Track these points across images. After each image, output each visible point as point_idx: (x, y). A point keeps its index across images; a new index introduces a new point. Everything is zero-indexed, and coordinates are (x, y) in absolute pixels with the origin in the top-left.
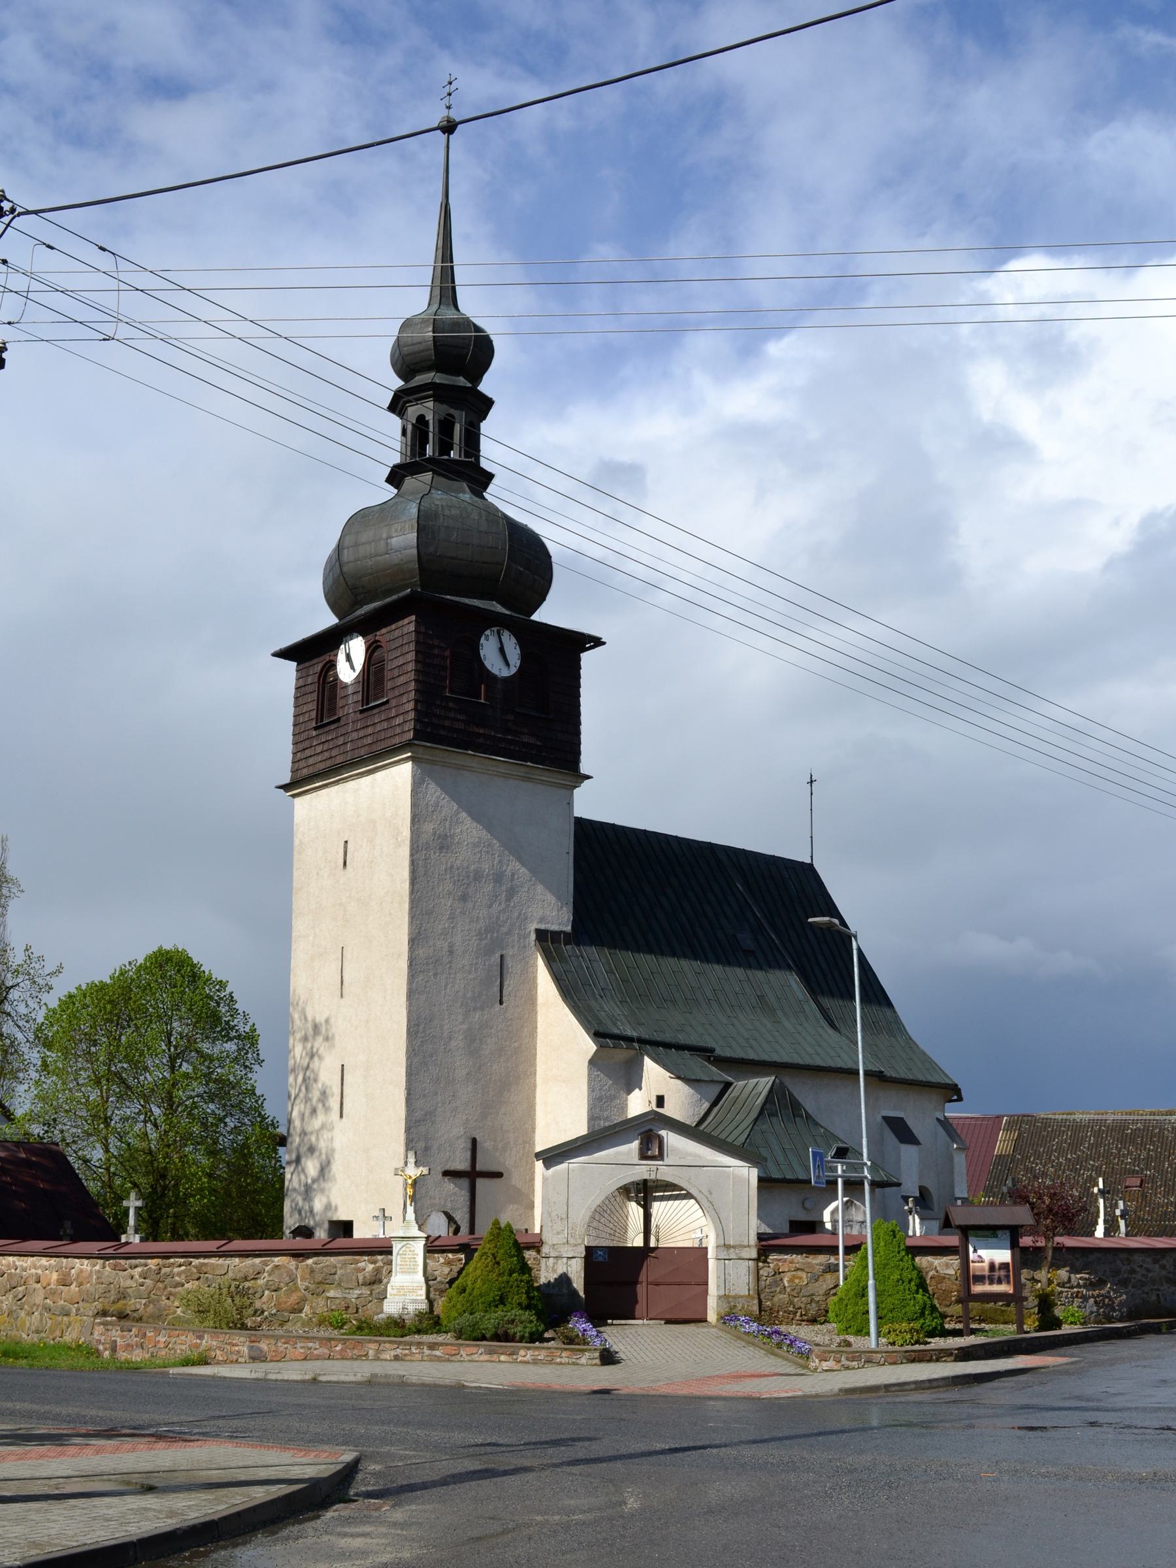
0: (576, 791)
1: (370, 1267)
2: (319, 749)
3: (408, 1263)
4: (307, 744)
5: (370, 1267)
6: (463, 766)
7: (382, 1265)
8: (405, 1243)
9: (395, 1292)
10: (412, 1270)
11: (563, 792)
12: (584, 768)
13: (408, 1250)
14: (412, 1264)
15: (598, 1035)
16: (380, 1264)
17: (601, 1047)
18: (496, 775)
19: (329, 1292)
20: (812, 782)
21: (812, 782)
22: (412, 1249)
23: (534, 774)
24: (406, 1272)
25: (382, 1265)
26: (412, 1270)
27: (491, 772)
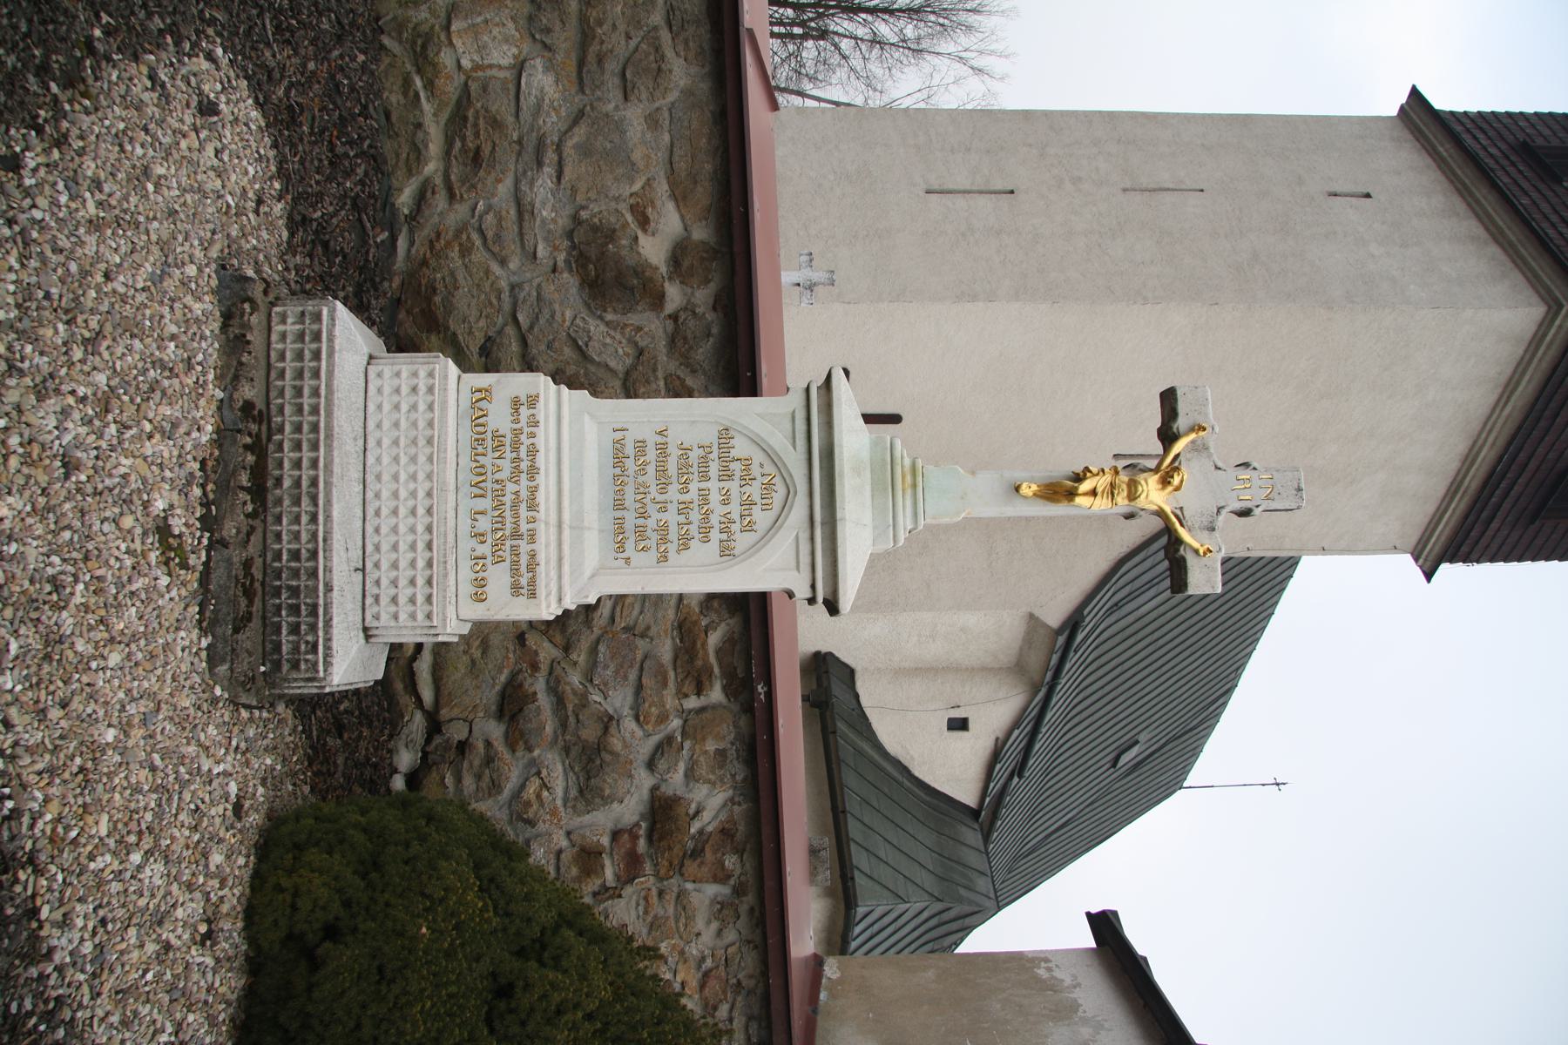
0: (1408, 558)
1: (654, 250)
2: (1493, 150)
3: (673, 493)
4: (1491, 133)
5: (654, 250)
6: (1512, 393)
7: (670, 307)
8: (794, 461)
9: (499, 418)
10: (631, 519)
11: (1413, 540)
12: (1445, 569)
13: (755, 490)
14: (672, 517)
15: (1073, 623)
16: (674, 295)
17: (1059, 632)
18: (1475, 442)
19: (547, 70)
20: (1278, 784)
21: (1278, 784)
22: (762, 518)
23: (1460, 501)
24: (619, 480)
25: (670, 307)
26: (631, 519)
27: (1484, 436)
